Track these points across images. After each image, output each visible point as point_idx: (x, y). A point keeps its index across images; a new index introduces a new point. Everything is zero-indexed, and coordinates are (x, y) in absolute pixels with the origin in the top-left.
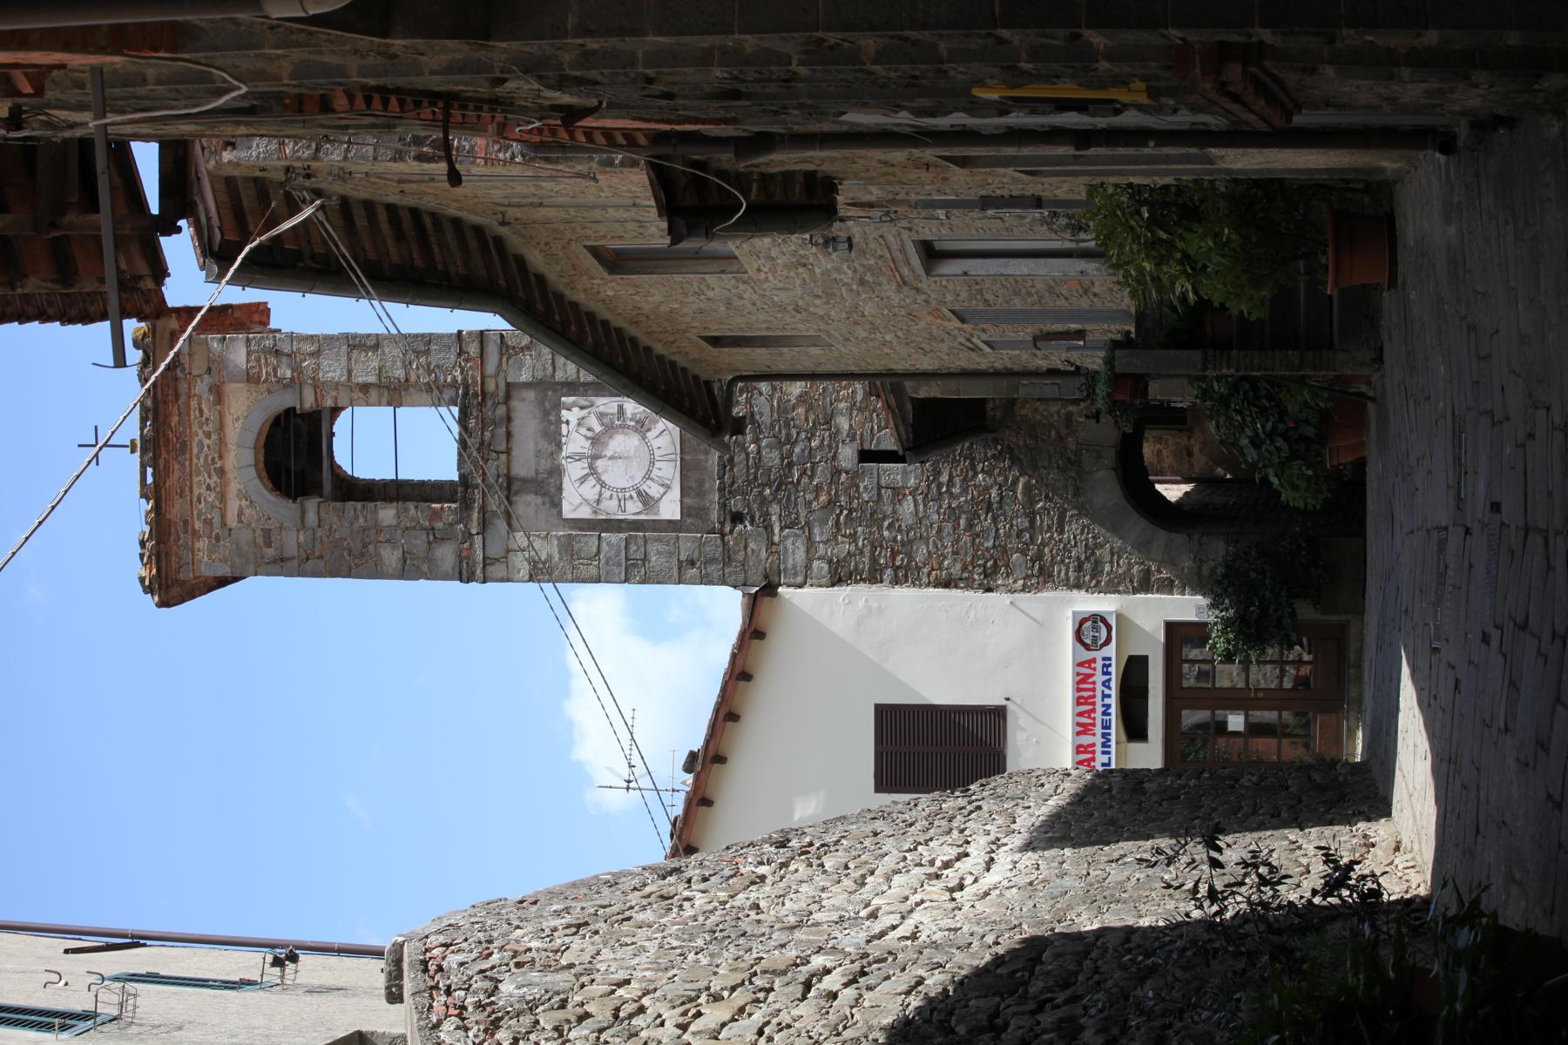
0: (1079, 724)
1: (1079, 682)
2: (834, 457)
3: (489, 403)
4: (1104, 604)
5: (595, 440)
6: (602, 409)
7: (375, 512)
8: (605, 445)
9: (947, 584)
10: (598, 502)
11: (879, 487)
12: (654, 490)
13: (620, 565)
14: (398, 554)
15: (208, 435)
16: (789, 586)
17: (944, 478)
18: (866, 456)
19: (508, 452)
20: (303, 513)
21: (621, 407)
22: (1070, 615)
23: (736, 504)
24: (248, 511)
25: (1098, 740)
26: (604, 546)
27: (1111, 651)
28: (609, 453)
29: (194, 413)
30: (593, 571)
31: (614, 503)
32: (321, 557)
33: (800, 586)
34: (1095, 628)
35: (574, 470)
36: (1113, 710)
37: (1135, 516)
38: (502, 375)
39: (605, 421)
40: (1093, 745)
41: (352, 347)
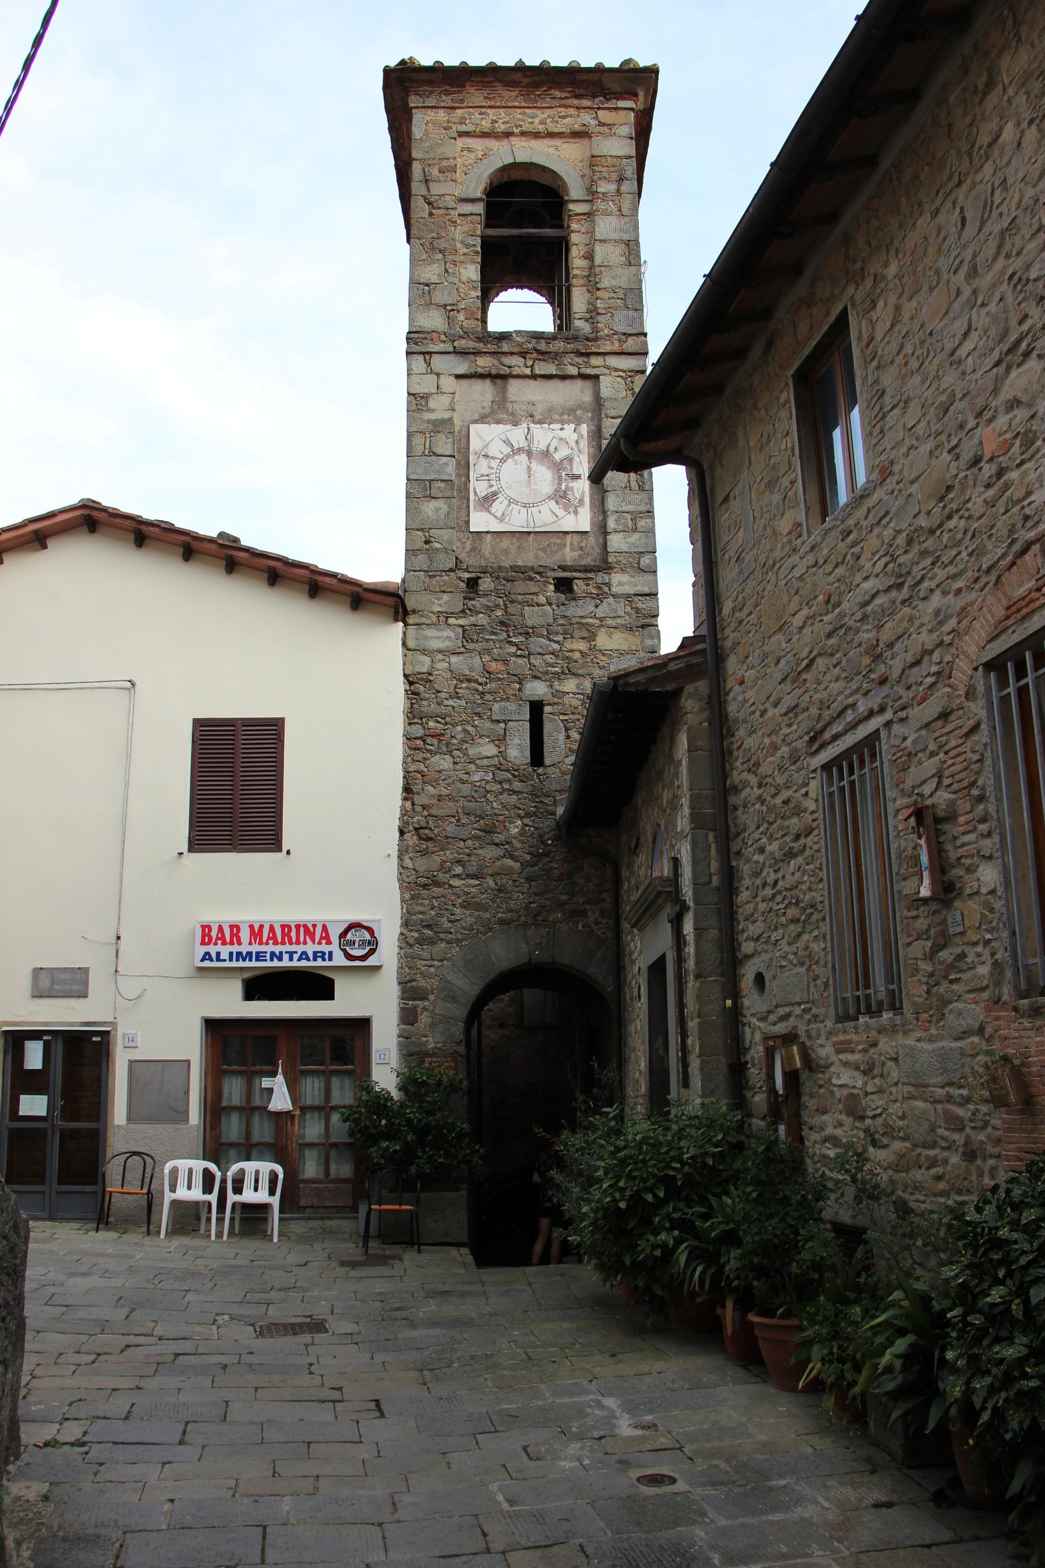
0: (261, 927)
1: (305, 926)
2: (536, 677)
3: (580, 360)
4: (388, 954)
5: (546, 455)
6: (576, 460)
7: (474, 262)
8: (541, 463)
9: (407, 789)
10: (486, 456)
11: (506, 722)
12: (498, 507)
13: (426, 473)
14: (435, 279)
15: (541, 123)
16: (404, 633)
17: (517, 785)
18: (537, 708)
19: (534, 377)
20: (473, 201)
21: (577, 477)
22: (377, 917)
23: (486, 584)
24: (472, 156)
25: (244, 948)
26: (444, 460)
27: (339, 960)
28: (534, 465)
29: (563, 111)
30: (419, 450)
31: (486, 471)
32: (431, 214)
33: (404, 644)
34: (363, 943)
35: (517, 435)
36: (276, 963)
37: (481, 985)
38: (607, 371)
39: (566, 463)
40: (239, 943)
41: (627, 243)
